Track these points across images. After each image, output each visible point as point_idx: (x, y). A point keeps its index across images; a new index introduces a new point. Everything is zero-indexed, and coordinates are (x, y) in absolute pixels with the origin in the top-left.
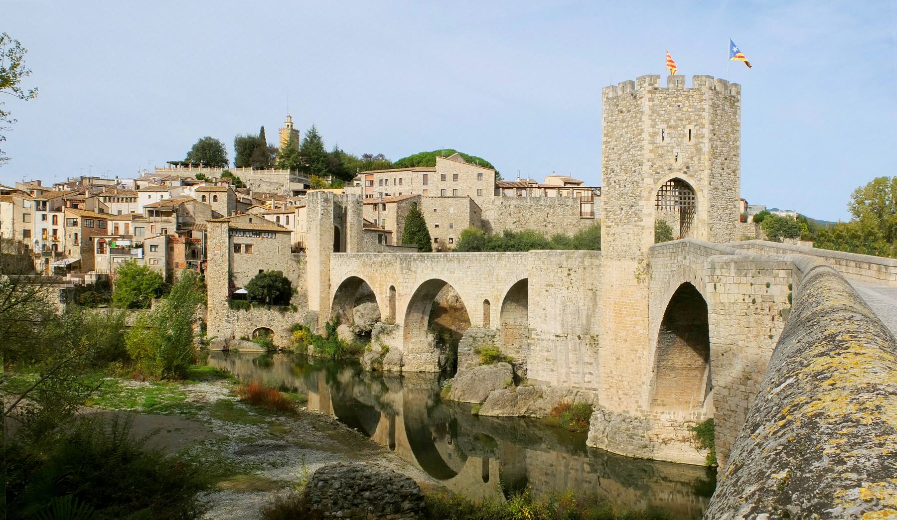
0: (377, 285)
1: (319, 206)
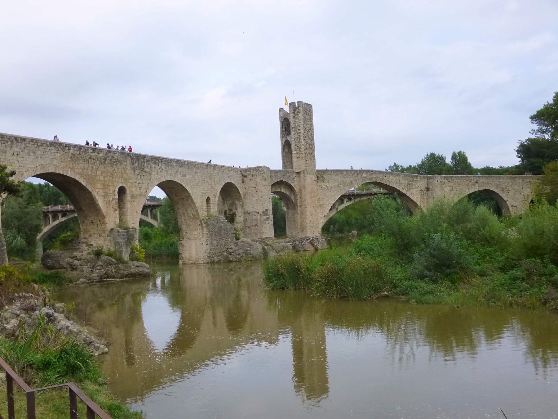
0: (99, 186)
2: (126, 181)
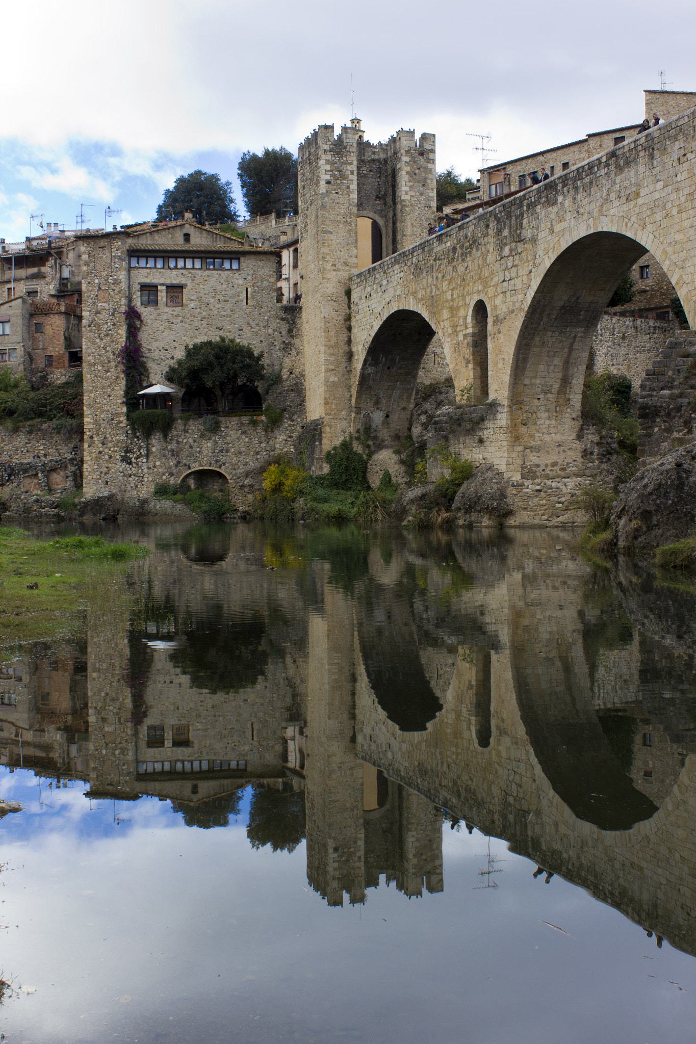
0: (445, 314)
1: (322, 162)
2: (486, 285)
